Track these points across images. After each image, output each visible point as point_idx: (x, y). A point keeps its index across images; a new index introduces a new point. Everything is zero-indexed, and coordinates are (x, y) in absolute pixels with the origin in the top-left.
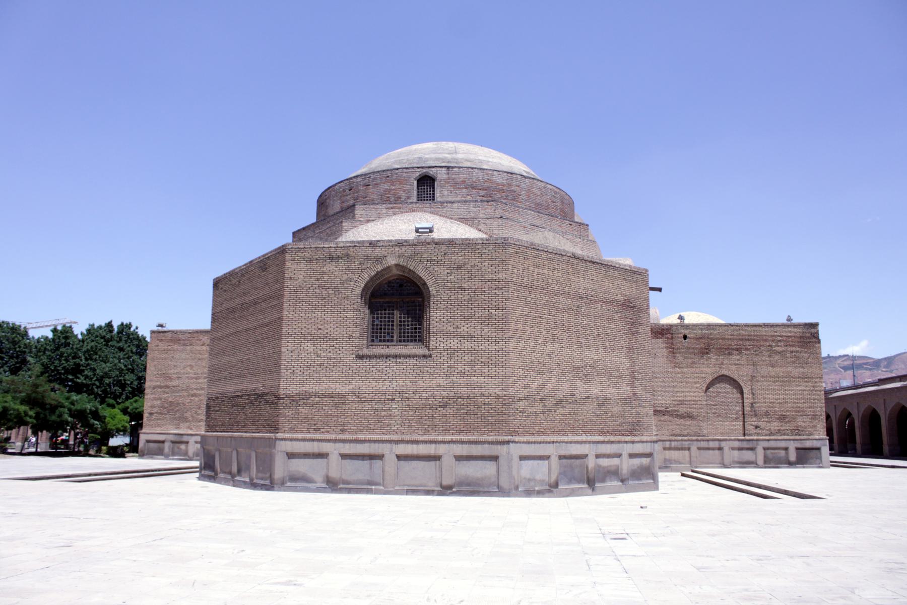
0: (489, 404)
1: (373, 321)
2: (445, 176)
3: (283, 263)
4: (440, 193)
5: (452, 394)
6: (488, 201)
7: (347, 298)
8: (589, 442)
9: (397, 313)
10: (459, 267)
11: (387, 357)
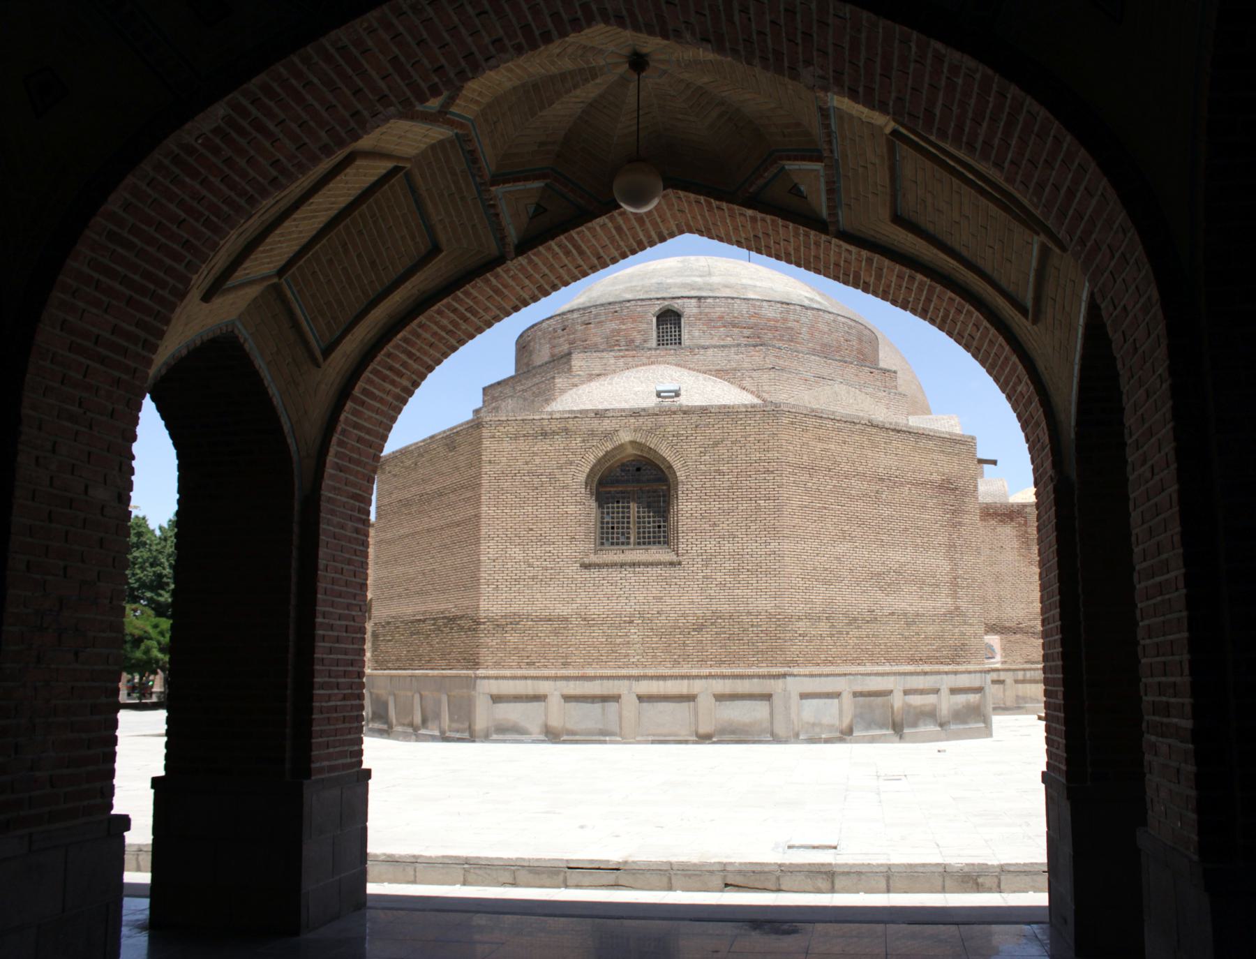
0: (758, 626)
1: (602, 518)
2: (695, 310)
3: (480, 441)
4: (690, 333)
5: (709, 614)
6: (755, 346)
7: (565, 487)
8: (895, 674)
9: (634, 507)
10: (716, 444)
11: (622, 565)
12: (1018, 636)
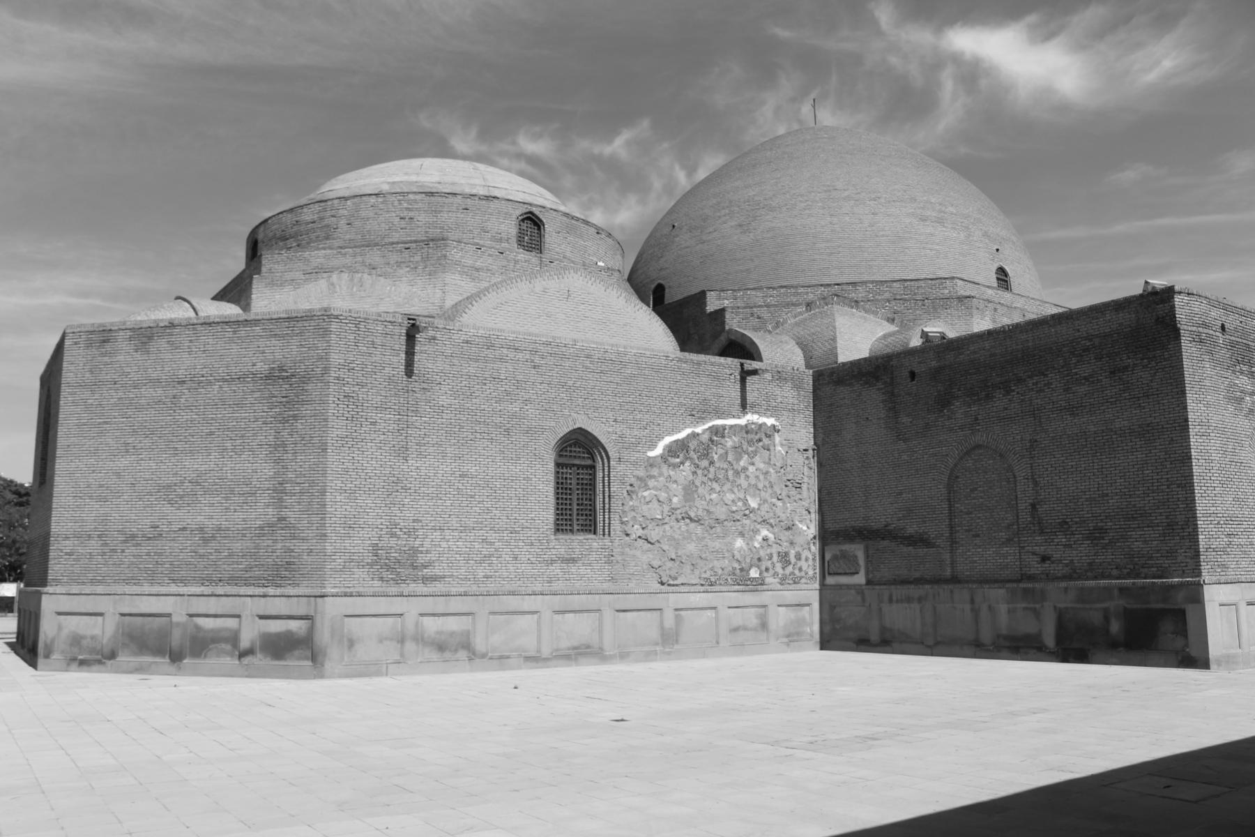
12: (886, 543)
